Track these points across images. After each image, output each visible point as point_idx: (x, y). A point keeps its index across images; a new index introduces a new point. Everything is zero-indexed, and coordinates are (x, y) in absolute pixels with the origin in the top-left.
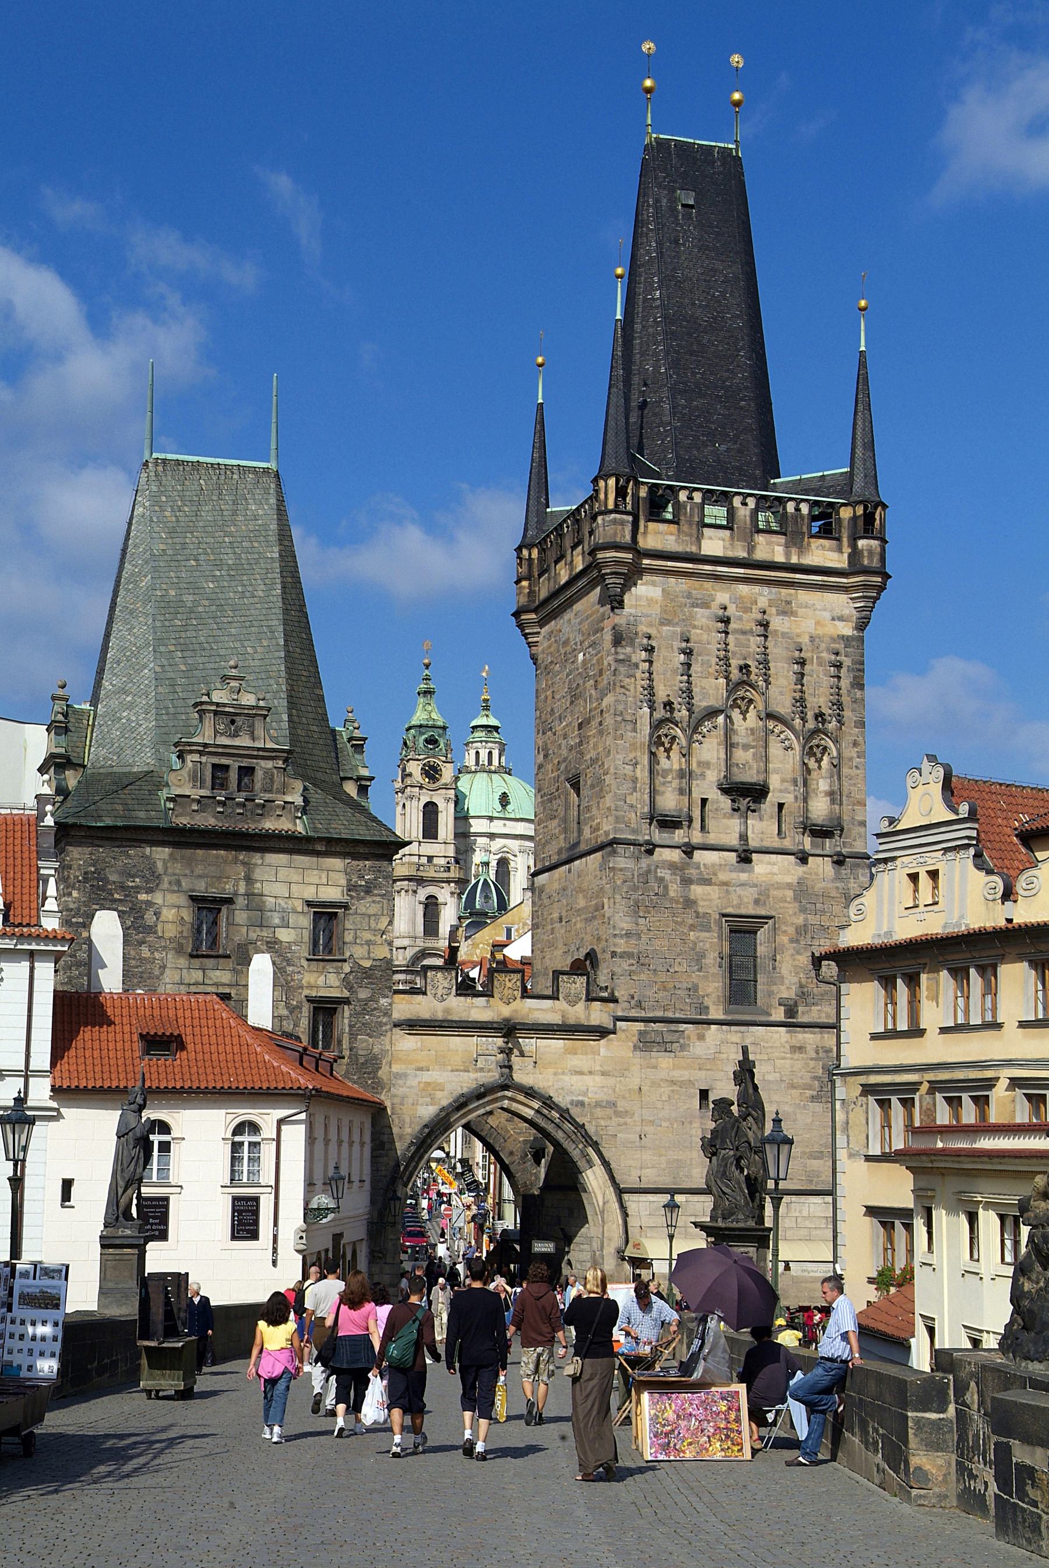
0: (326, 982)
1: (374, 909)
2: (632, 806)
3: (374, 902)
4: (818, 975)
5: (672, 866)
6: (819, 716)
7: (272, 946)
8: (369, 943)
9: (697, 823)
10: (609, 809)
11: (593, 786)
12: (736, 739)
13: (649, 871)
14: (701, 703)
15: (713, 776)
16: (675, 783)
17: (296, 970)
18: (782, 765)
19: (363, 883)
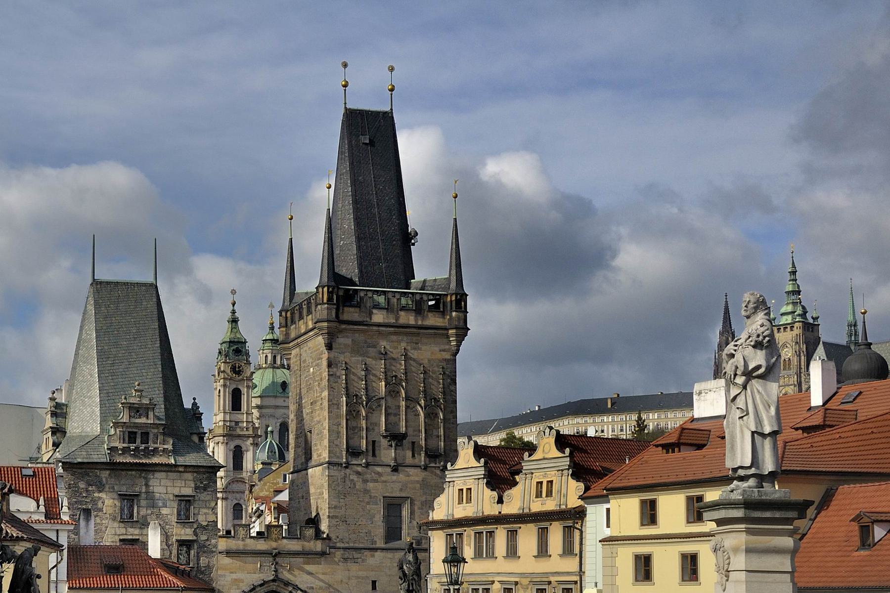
0: (187, 533)
7: (159, 516)
8: (205, 514)
9: (371, 453)
11: (318, 434)
12: (390, 411)
13: (345, 477)
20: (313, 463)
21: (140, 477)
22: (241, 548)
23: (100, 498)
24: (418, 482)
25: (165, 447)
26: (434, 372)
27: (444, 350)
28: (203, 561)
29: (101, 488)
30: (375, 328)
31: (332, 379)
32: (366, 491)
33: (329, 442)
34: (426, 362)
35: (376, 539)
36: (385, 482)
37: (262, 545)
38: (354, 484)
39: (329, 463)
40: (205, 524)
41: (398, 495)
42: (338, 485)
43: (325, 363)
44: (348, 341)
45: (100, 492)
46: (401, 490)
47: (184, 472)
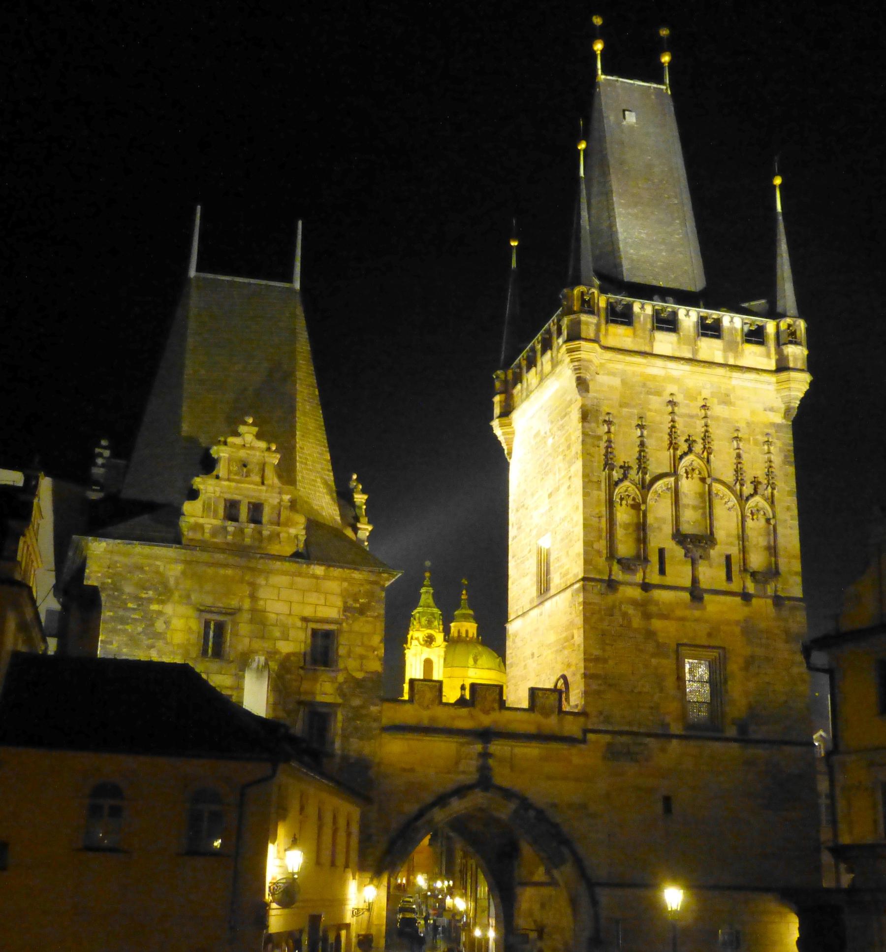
1: (367, 628)
2: (599, 552)
3: (367, 622)
4: (808, 663)
5: (634, 603)
6: (756, 483)
8: (362, 657)
10: (578, 555)
11: (562, 540)
12: (684, 500)
13: (613, 607)
14: (654, 468)
15: (668, 529)
16: (634, 536)
17: (294, 677)
18: (726, 522)
19: (358, 605)
20: (553, 591)
21: (242, 581)
22: (426, 723)
23: (160, 613)
24: (737, 623)
25: (293, 531)
26: (756, 443)
27: (772, 409)
28: (356, 745)
29: (165, 593)
30: (659, 362)
31: (589, 440)
32: (650, 634)
33: (587, 544)
34: (742, 425)
35: (668, 719)
36: (683, 619)
37: (464, 720)
38: (630, 622)
39: (584, 579)
40: (359, 675)
41: (706, 644)
42: (601, 620)
43: (575, 415)
44: (616, 382)
45: (161, 602)
46: (710, 635)
47: (326, 578)
